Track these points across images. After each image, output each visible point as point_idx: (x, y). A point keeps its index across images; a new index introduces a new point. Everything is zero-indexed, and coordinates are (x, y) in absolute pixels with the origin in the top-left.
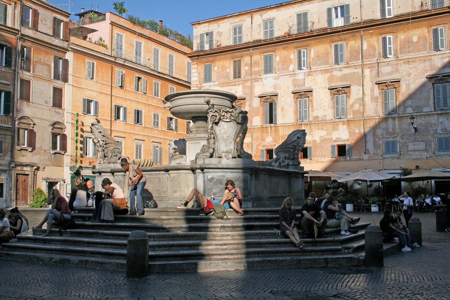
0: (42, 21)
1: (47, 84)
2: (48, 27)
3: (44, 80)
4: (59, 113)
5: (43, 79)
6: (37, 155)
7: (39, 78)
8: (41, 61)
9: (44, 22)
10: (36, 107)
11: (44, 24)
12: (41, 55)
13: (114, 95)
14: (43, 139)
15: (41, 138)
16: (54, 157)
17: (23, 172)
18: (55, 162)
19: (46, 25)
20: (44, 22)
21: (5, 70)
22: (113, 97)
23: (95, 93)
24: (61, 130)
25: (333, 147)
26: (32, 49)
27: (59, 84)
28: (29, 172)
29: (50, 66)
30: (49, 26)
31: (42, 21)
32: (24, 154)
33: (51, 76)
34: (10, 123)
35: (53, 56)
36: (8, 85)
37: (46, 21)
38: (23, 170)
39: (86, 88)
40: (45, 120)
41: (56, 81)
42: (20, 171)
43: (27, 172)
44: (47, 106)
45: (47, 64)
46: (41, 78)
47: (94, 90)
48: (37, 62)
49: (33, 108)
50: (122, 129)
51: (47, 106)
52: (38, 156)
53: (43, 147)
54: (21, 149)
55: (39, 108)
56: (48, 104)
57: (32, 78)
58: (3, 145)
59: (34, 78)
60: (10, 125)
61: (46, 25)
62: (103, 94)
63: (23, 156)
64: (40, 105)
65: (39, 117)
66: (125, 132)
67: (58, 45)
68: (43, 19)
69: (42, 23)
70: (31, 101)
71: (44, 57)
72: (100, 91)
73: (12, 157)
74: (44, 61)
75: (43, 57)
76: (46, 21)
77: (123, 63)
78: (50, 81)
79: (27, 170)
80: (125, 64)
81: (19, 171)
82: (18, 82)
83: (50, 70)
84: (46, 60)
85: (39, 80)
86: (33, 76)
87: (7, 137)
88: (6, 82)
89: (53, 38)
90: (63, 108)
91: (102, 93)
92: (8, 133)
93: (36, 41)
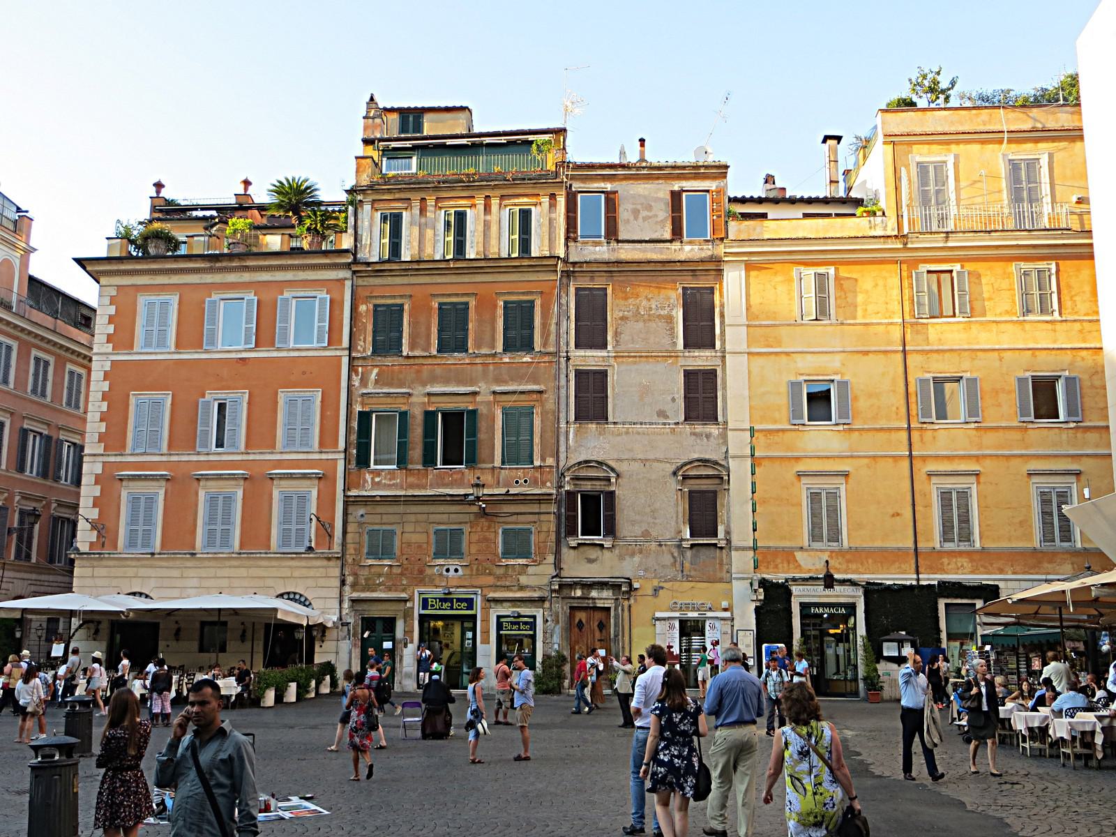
0: (636, 213)
1: (661, 367)
2: (657, 222)
3: (651, 360)
4: (708, 436)
5: (647, 357)
6: (633, 555)
7: (635, 357)
8: (639, 313)
9: (644, 213)
10: (627, 433)
11: (643, 218)
12: (638, 296)
13: (912, 348)
14: (652, 511)
15: (648, 510)
16: (694, 556)
17: (591, 601)
18: (695, 570)
19: (650, 217)
20: (644, 213)
21: (532, 358)
22: (909, 358)
23: (838, 357)
24: (717, 481)
25: (1021, 381)
26: (609, 291)
27: (701, 359)
28: (606, 601)
29: (670, 319)
30: (659, 219)
31: (636, 213)
32: (593, 556)
33: (675, 344)
34: (548, 484)
35: (680, 291)
36: (540, 392)
37: (649, 208)
38: (588, 599)
39: (800, 350)
40: (658, 461)
41: (692, 354)
42: (579, 601)
43: (602, 601)
44: (664, 424)
45: (660, 316)
46: (641, 357)
47: (835, 349)
48: (627, 318)
49: (619, 435)
50: (965, 449)
51: (664, 424)
52: (637, 559)
53: (654, 534)
54: (579, 544)
55: (638, 433)
56: (667, 417)
57: (612, 361)
58: (533, 538)
59: (620, 360)
60: (549, 488)
61: (650, 217)
62: (870, 354)
63: (590, 561)
64: (641, 424)
65: (640, 456)
66: (977, 458)
67: (695, 259)
68: (639, 207)
69: (636, 218)
70: (610, 419)
71: (649, 300)
72: (855, 349)
73: (558, 565)
74: (650, 309)
75: (644, 303)
76: (649, 208)
77: (941, 245)
78: (671, 355)
79: (603, 598)
80: (950, 244)
81: (576, 601)
82: (568, 381)
83: (672, 330)
84: (654, 307)
85: (635, 363)
86: (615, 357)
87: (543, 517)
88: (536, 387)
89: (676, 246)
90: (720, 419)
91: (866, 353)
92: (544, 508)
93: (615, 268)
